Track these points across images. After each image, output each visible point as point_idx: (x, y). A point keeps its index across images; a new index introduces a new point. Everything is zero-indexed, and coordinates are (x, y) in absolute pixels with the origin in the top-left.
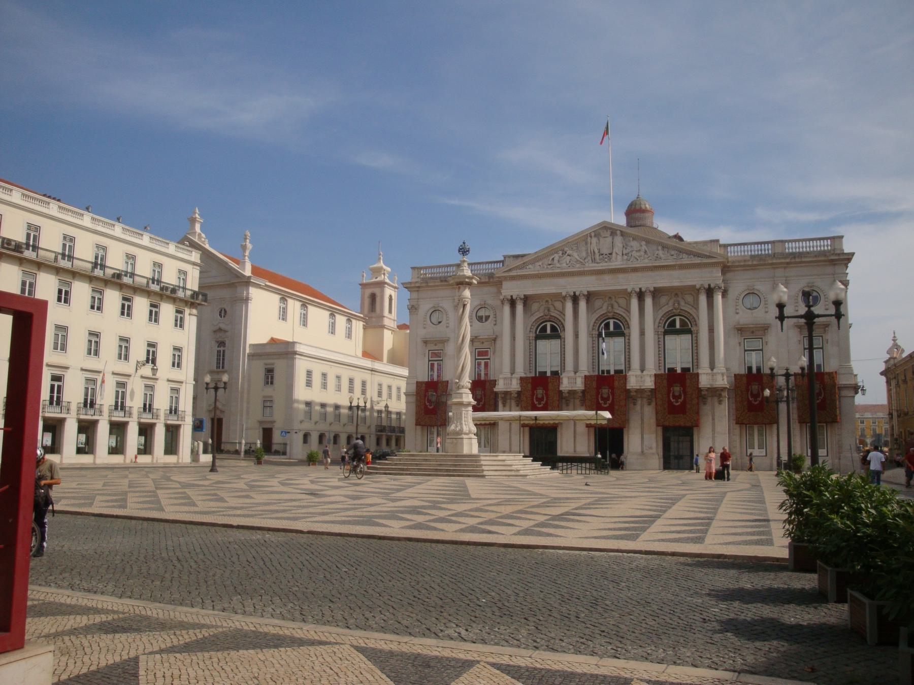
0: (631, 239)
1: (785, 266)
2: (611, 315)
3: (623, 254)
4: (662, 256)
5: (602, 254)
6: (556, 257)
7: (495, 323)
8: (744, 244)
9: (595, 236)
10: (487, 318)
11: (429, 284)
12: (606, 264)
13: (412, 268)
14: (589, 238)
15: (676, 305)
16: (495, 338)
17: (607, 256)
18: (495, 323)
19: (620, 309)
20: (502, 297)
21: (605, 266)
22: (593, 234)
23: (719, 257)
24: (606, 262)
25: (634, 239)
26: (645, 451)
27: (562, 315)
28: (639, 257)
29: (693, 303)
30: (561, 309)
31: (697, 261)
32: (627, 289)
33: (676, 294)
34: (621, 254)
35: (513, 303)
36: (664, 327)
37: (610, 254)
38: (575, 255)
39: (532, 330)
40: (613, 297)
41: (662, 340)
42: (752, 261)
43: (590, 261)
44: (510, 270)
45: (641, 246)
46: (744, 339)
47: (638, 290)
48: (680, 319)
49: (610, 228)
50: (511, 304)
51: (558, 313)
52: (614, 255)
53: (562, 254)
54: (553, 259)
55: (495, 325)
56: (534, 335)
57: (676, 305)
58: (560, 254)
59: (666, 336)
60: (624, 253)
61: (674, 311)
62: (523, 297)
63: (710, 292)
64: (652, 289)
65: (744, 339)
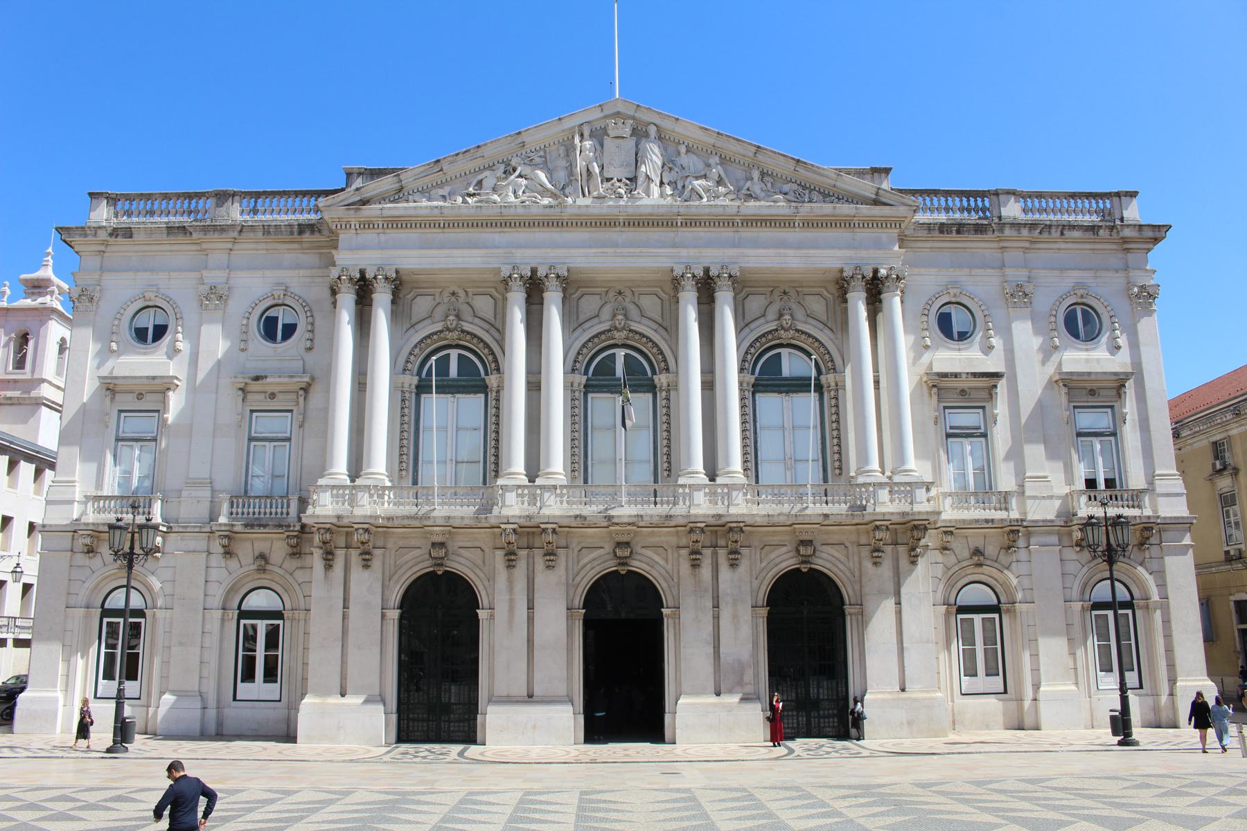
0: (683, 149)
1: (1027, 245)
2: (619, 336)
5: (608, 180)
7: (308, 344)
8: (935, 192)
9: (591, 136)
10: (289, 330)
13: (91, 194)
14: (577, 140)
16: (309, 385)
18: (308, 344)
19: (645, 321)
25: (689, 150)
29: (825, 318)
30: (489, 315)
33: (785, 293)
35: (364, 289)
36: (753, 373)
39: (409, 366)
40: (628, 293)
41: (749, 402)
44: (365, 202)
45: (709, 166)
47: (700, 273)
49: (633, 118)
50: (358, 294)
51: (486, 326)
53: (505, 172)
54: (480, 183)
55: (310, 349)
56: (415, 380)
57: (787, 317)
59: (758, 396)
60: (665, 180)
63: (875, 290)
65: (945, 408)
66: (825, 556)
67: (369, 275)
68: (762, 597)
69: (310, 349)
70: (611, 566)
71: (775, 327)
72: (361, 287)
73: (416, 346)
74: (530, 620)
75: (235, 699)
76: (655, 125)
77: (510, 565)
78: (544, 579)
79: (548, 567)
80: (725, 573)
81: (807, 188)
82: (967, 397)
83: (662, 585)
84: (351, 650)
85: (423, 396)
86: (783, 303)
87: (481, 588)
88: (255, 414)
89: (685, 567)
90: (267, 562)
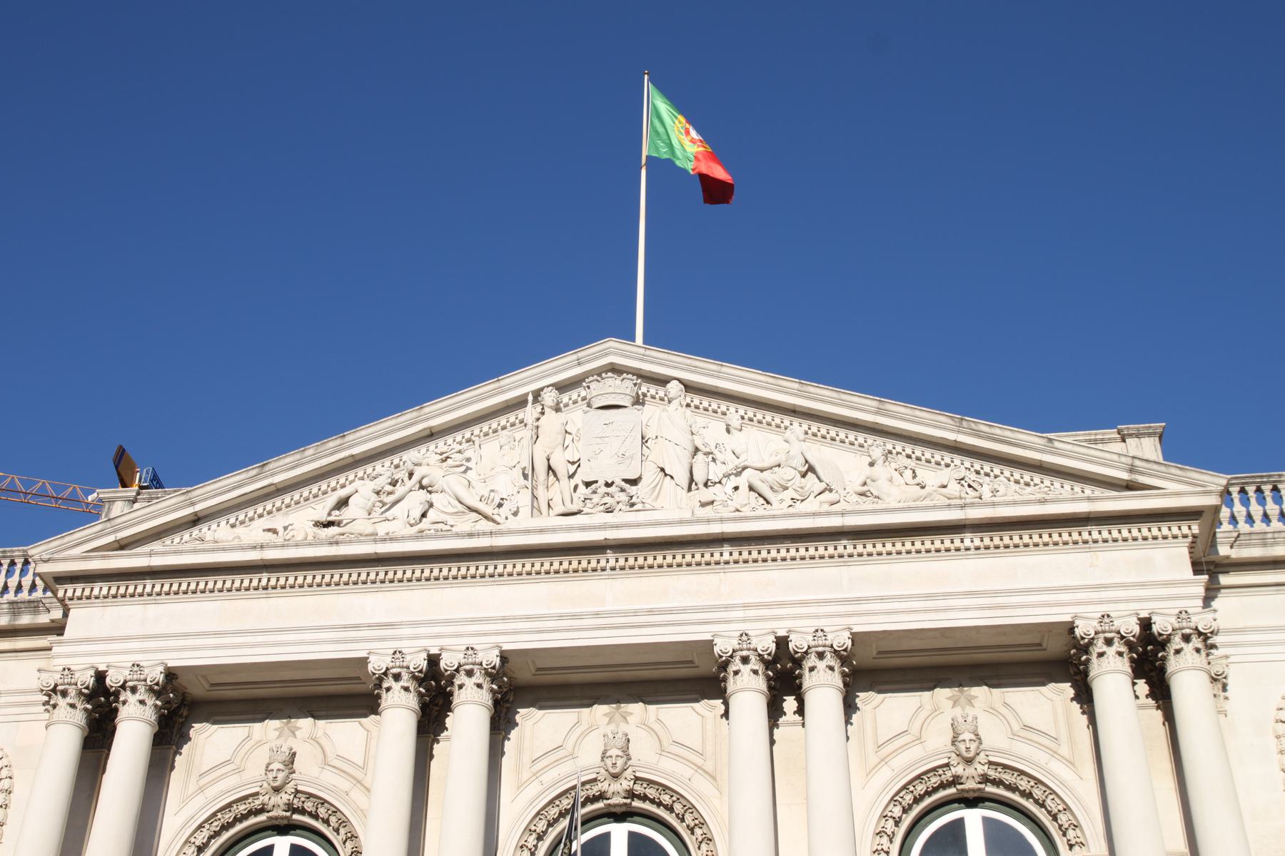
3: (692, 480)
5: (588, 484)
12: (609, 518)
15: (967, 736)
17: (609, 490)
20: (51, 679)
24: (609, 511)
27: (357, 795)
31: (1069, 500)
32: (710, 644)
34: (686, 486)
37: (624, 480)
43: (525, 511)
52: (650, 476)
54: (343, 503)
58: (382, 482)
60: (699, 477)
61: (959, 770)
62: (157, 675)
64: (842, 640)
67: (112, 680)
71: (946, 761)
72: (97, 707)
73: (201, 826)
76: (680, 381)
81: (987, 475)
86: (958, 712)
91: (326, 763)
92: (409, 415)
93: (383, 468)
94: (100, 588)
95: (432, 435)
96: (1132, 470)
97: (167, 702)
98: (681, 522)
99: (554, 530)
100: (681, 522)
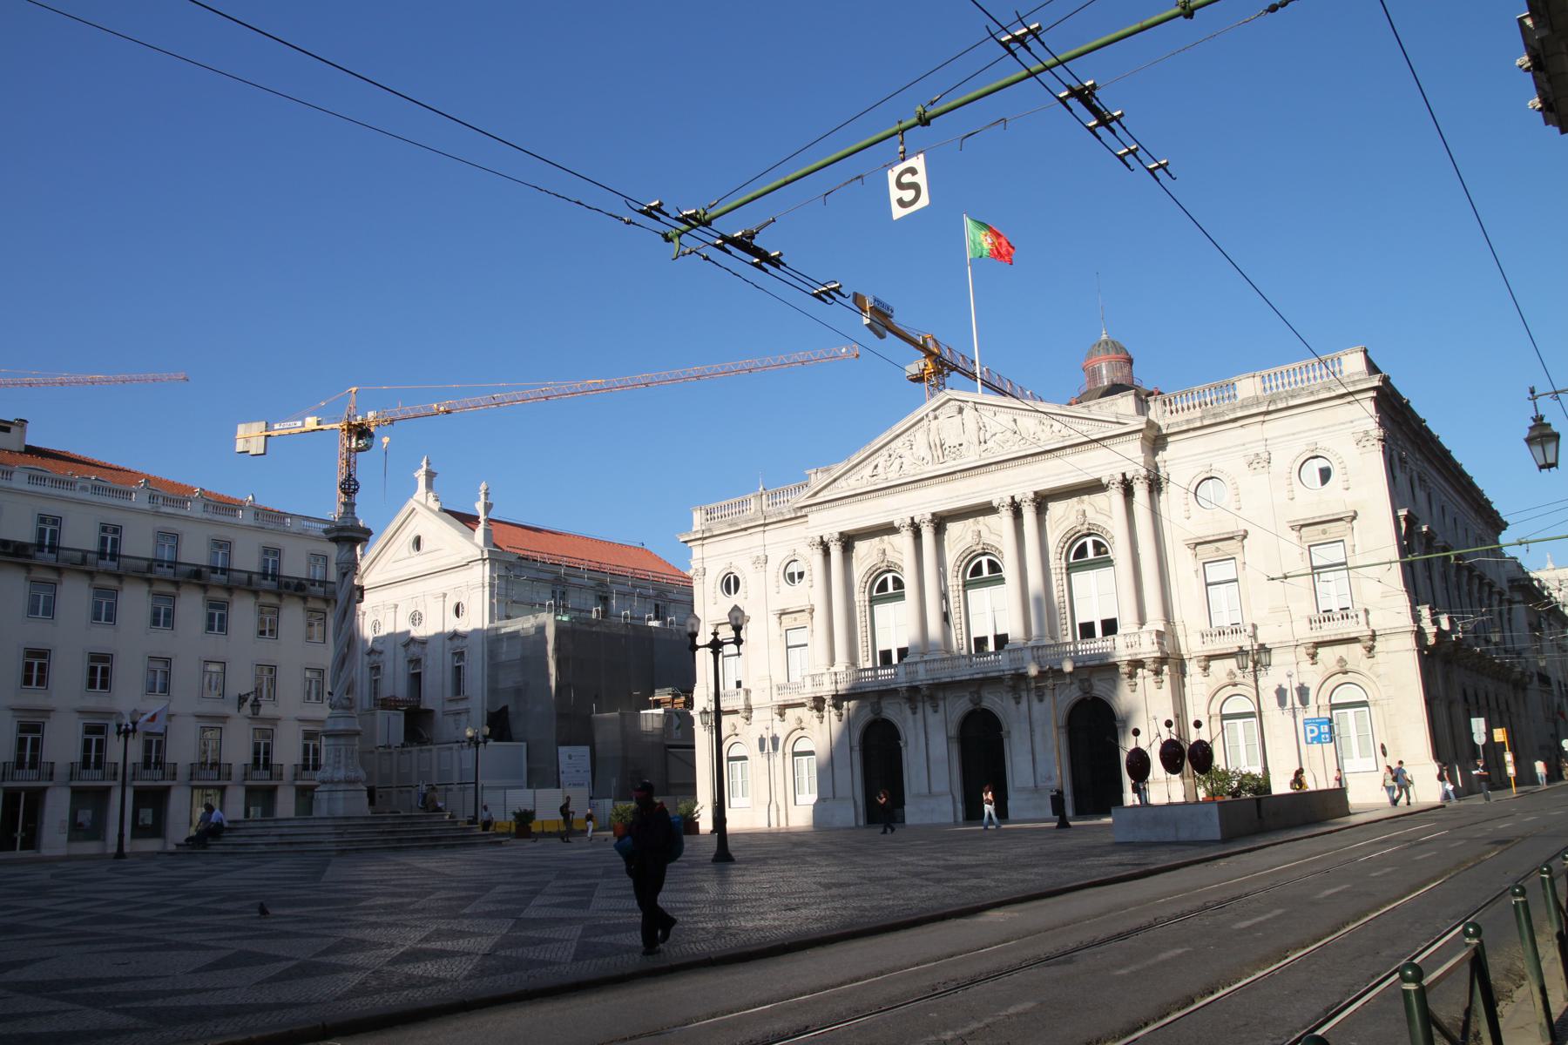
3: (980, 443)
4: (1043, 436)
6: (880, 459)
7: (810, 583)
10: (801, 575)
11: (715, 533)
12: (954, 463)
17: (955, 449)
18: (810, 583)
21: (953, 466)
22: (931, 416)
23: (1132, 422)
24: (955, 459)
26: (1040, 784)
28: (1004, 443)
34: (977, 443)
38: (906, 453)
42: (1202, 420)
44: (816, 493)
46: (1204, 564)
48: (1095, 542)
54: (876, 467)
55: (811, 586)
60: (982, 440)
63: (1128, 489)
66: (1100, 688)
68: (1062, 721)
69: (811, 586)
70: (970, 707)
74: (927, 745)
75: (795, 804)
77: (914, 713)
78: (935, 720)
79: (936, 712)
80: (1036, 705)
82: (1220, 552)
83: (1001, 716)
84: (836, 771)
85: (875, 607)
87: (901, 728)
88: (788, 632)
89: (1013, 702)
90: (801, 722)
91: (895, 551)
92: (888, 432)
93: (884, 452)
94: (814, 508)
95: (898, 436)
96: (1117, 418)
97: (843, 542)
98: (976, 461)
99: (938, 470)
100: (976, 461)
